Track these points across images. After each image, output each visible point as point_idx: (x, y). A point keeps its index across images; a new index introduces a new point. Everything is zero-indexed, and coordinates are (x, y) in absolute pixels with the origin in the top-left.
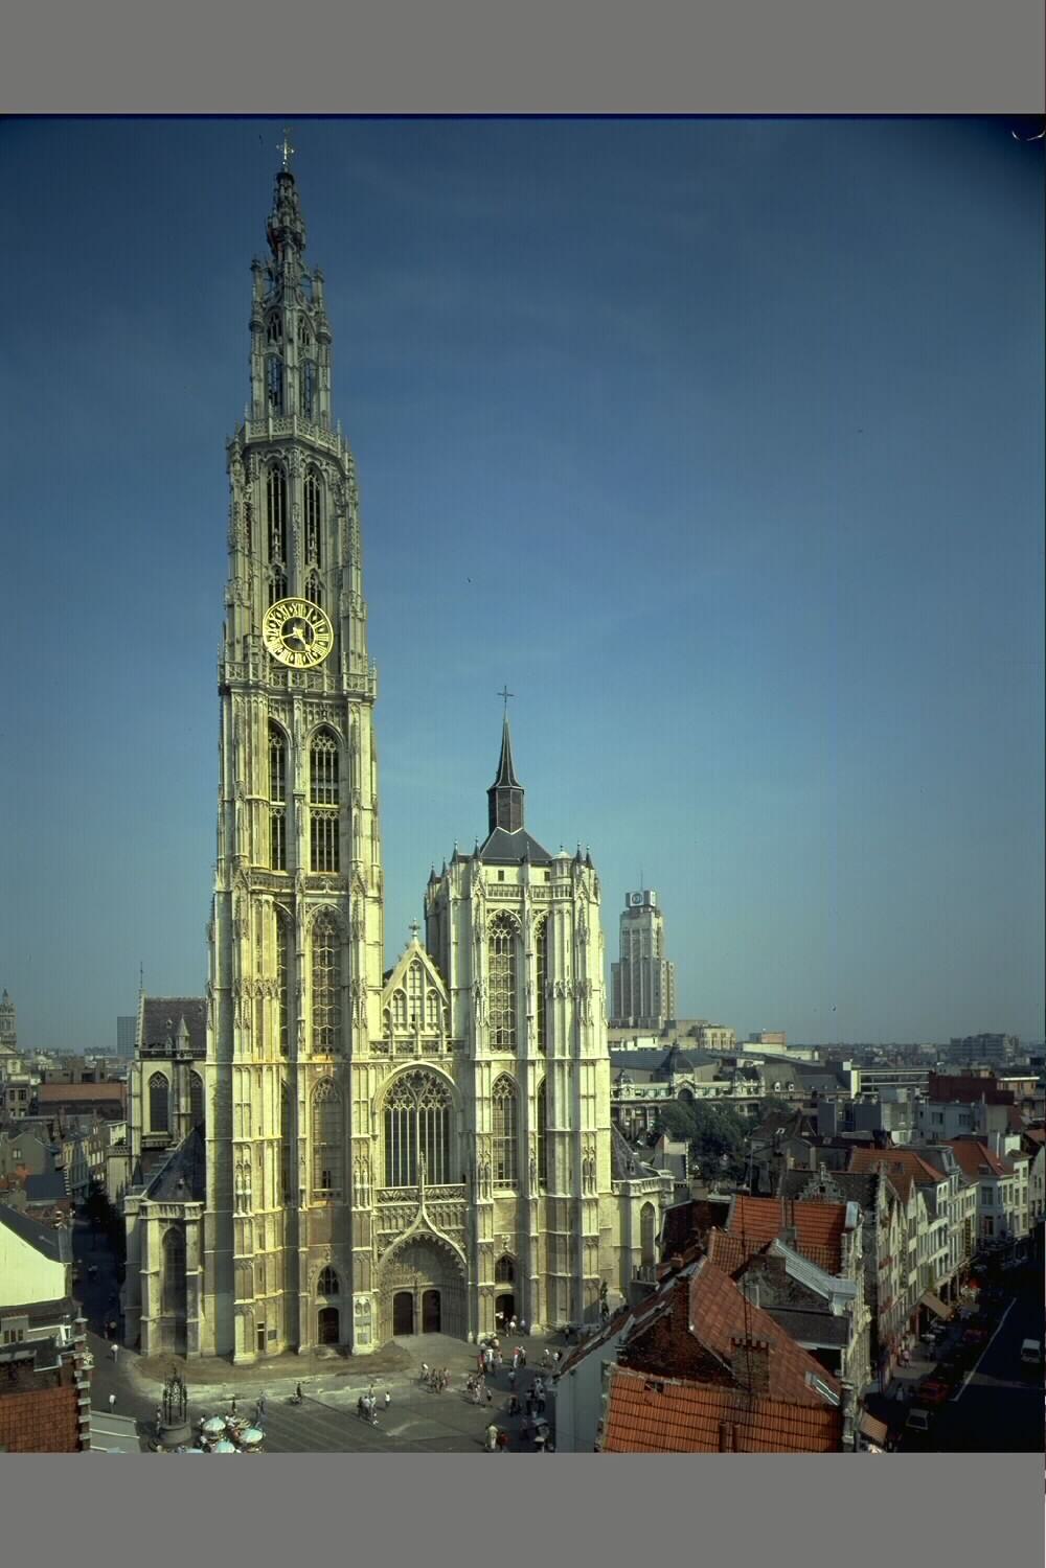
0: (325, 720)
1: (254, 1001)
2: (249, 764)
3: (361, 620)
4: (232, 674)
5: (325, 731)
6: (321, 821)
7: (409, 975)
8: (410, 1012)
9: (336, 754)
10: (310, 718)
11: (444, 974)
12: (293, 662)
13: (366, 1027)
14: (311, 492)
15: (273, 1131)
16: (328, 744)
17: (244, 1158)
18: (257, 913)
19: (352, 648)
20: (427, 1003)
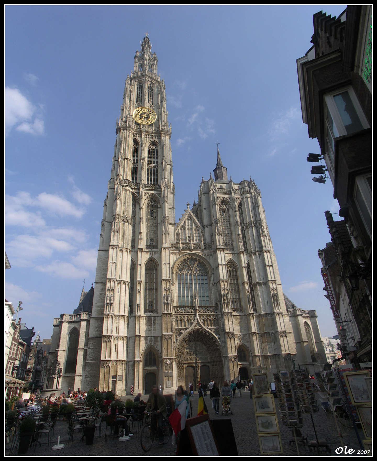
0: (153, 139)
1: (121, 224)
2: (125, 149)
3: (166, 115)
4: (121, 124)
5: (153, 143)
6: (151, 169)
7: (187, 221)
8: (187, 235)
9: (157, 150)
10: (148, 139)
11: (201, 221)
12: (143, 123)
13: (168, 234)
14: (151, 89)
15: (127, 277)
16: (154, 147)
17: (112, 286)
18: (124, 194)
19: (163, 120)
20: (194, 232)
